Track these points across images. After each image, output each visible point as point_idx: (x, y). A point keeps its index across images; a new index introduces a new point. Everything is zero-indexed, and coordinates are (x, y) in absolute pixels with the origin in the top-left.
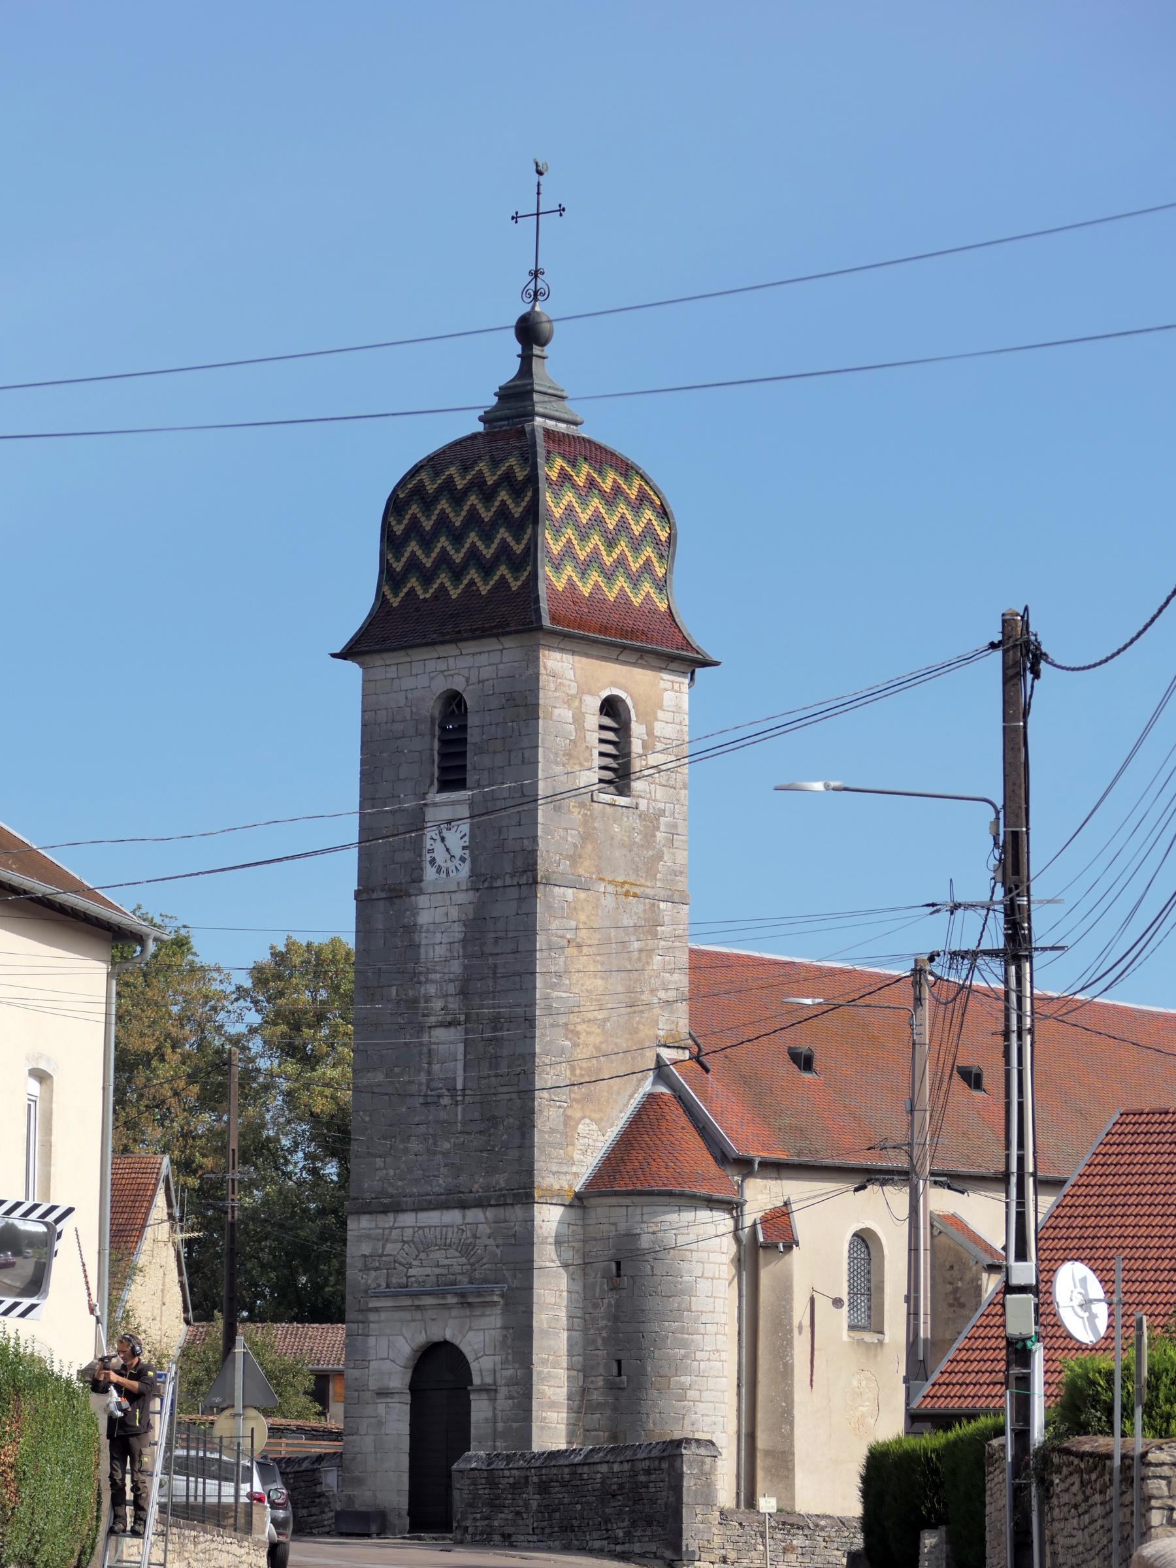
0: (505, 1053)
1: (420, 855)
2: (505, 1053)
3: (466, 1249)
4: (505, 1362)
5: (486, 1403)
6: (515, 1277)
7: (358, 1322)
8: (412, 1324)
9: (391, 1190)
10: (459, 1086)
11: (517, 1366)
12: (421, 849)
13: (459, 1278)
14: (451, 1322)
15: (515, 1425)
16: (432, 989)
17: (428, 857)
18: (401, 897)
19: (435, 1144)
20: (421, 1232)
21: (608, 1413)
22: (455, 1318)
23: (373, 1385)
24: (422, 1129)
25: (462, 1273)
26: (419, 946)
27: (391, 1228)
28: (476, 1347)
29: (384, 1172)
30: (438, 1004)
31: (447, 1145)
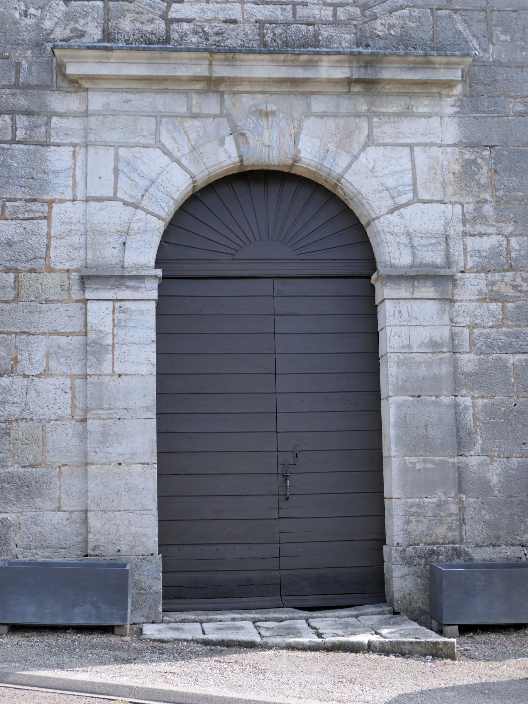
5: (432, 307)
6: (489, 36)
7: (12, 113)
8: (189, 123)
11: (510, 228)
13: (325, 32)
14: (309, 124)
15: (512, 359)
22: (323, 115)
23: (65, 256)
25: (336, 23)
28: (390, 182)
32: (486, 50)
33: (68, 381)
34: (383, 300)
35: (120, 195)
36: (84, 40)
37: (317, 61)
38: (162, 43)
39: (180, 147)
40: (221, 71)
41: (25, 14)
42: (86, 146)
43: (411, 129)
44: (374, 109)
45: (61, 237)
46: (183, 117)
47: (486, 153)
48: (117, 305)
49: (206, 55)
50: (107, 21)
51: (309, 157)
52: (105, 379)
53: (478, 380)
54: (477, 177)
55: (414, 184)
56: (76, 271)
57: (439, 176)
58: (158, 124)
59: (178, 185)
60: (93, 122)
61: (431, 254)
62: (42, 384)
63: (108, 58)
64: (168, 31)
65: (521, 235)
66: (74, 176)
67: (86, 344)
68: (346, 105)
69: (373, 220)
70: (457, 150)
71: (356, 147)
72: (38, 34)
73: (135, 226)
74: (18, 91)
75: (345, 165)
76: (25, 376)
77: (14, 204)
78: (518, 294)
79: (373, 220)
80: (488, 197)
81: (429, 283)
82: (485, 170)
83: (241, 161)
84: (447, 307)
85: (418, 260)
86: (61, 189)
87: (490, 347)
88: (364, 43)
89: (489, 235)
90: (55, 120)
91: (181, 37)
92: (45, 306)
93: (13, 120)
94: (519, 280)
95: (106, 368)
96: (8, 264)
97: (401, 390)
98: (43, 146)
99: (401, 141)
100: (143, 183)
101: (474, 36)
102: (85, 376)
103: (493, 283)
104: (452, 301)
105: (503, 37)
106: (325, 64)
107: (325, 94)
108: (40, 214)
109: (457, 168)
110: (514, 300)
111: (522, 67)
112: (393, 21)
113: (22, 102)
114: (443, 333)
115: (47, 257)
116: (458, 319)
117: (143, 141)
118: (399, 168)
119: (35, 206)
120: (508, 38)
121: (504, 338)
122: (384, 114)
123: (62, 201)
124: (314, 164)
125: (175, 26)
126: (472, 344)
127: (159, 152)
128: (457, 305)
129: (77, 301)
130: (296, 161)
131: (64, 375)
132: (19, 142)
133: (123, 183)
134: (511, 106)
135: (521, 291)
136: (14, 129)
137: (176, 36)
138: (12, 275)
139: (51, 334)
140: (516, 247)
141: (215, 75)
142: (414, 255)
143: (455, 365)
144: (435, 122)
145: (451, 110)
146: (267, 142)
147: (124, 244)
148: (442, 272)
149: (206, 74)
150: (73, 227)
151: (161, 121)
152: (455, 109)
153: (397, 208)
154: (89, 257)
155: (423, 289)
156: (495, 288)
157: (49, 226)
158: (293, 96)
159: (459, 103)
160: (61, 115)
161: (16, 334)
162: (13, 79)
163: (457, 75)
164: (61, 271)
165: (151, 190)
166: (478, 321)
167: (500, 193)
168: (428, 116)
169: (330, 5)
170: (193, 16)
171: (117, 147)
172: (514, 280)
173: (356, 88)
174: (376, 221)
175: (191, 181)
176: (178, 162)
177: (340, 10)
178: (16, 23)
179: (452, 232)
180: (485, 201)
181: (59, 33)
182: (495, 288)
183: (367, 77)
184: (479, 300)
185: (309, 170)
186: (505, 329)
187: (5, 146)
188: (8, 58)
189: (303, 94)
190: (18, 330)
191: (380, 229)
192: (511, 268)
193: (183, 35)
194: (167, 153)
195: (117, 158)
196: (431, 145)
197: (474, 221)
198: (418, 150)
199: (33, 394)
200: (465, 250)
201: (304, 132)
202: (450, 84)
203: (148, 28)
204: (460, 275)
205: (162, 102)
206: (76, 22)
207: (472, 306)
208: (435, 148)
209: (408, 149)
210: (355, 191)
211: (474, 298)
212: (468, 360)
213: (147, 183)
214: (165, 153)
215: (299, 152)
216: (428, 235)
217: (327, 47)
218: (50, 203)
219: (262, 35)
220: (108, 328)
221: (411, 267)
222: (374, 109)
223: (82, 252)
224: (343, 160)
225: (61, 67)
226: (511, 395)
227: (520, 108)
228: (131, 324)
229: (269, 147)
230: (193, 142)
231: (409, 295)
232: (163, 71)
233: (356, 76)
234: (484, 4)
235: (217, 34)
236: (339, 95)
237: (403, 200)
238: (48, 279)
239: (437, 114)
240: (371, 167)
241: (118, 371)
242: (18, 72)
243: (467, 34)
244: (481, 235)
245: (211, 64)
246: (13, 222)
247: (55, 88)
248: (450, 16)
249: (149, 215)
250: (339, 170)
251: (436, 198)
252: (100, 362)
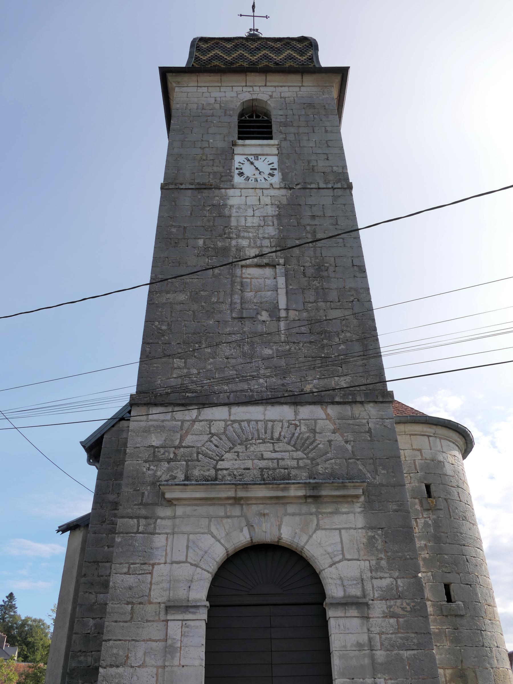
0: (334, 286)
1: (230, 170)
2: (334, 286)
3: (301, 444)
4: (376, 569)
5: (356, 622)
6: (376, 472)
7: (138, 517)
8: (225, 521)
9: (192, 387)
10: (282, 304)
11: (396, 574)
13: (293, 472)
14: (286, 519)
16: (245, 243)
17: (237, 172)
18: (210, 189)
19: (252, 348)
20: (236, 425)
21: (447, 645)
22: (293, 515)
23: (158, 595)
25: (298, 467)
26: (230, 216)
27: (194, 421)
28: (330, 550)
29: (185, 371)
31: (268, 352)
32: (375, 478)
33: (155, 670)
34: (329, 618)
35: (189, 560)
36: (176, 480)
37: (288, 487)
38: (214, 481)
39: (220, 533)
40: (241, 494)
41: (149, 469)
42: (173, 534)
43: (339, 520)
44: (319, 510)
45: (157, 584)
46: (222, 517)
47: (380, 532)
48: (184, 623)
49: (234, 486)
50: (187, 471)
51: (286, 537)
52: (175, 669)
54: (376, 545)
55: (343, 550)
56: (164, 603)
57: (355, 546)
58: (210, 521)
59: (219, 554)
60: (177, 521)
61: (354, 589)
62: (141, 672)
63: (186, 489)
64: (216, 475)
65: (403, 578)
66: (166, 550)
67: (166, 647)
68: (305, 509)
69: (322, 571)
70: (364, 531)
71: (311, 531)
72: (154, 479)
73: (196, 577)
74: (141, 507)
75: (305, 541)
76: (132, 667)
77: (134, 566)
78: (405, 613)
79: (322, 571)
80: (382, 556)
81: (354, 607)
82: (380, 541)
83: (252, 540)
84: (365, 622)
85: (347, 594)
86: (159, 557)
87: (392, 646)
88: (313, 477)
89: (385, 578)
90: (159, 521)
91: (223, 477)
92: (146, 624)
93: (138, 521)
94: (405, 604)
95: (176, 662)
96: (128, 600)
97: (342, 675)
98: (152, 534)
99: (334, 527)
100: (201, 553)
101: (368, 471)
102: (164, 667)
103: (390, 607)
104: (368, 618)
105: (383, 472)
106: (292, 489)
107: (294, 503)
108: (148, 571)
109: (365, 540)
110: (403, 616)
111: (394, 486)
112: (327, 465)
113: (143, 512)
114: (364, 638)
115: (149, 595)
116: (373, 629)
117: (202, 531)
118: (334, 542)
119: (145, 567)
120: (385, 472)
121: (400, 641)
122: (324, 513)
123: (159, 564)
124: (289, 541)
125: (220, 472)
126: (382, 645)
127: (209, 536)
128: (371, 620)
129: (163, 621)
130: (280, 539)
131: (153, 666)
132: (140, 533)
133: (191, 554)
134: (390, 506)
135: (406, 611)
136: (139, 526)
137: (220, 477)
138: (130, 606)
139: (148, 641)
140: (401, 585)
141: (238, 496)
142: (345, 591)
143: (372, 658)
144: (351, 516)
145: (359, 510)
146: (264, 530)
147: (190, 587)
148: (361, 601)
149: (233, 495)
150: (164, 578)
151: (211, 520)
152: (361, 509)
153: (334, 564)
154: (171, 595)
155: (351, 611)
156: (392, 610)
157: (152, 578)
158: (277, 505)
159: (363, 506)
160: (162, 518)
161: (129, 641)
162: (140, 501)
163: (360, 492)
164: (156, 603)
165: (205, 557)
166: (384, 630)
167: (389, 554)
168: (347, 513)
169: (295, 459)
170: (229, 467)
171: (189, 534)
172: (402, 605)
173: (309, 500)
174: (323, 572)
175: (225, 552)
176: (219, 541)
177: (300, 461)
178: (144, 473)
179: (365, 577)
180: (382, 559)
181: (164, 478)
182: (392, 610)
183: (314, 494)
184: (383, 617)
185: (287, 544)
186: (400, 635)
187: (133, 535)
188: (138, 490)
189: (283, 504)
190: (131, 639)
191: (325, 576)
192: (399, 597)
193: (224, 476)
194: (214, 537)
195: (188, 540)
196: (350, 528)
197: (376, 570)
198: (343, 531)
199: (135, 678)
200: (373, 587)
201: (284, 523)
202: (357, 497)
203: (207, 473)
204: (371, 602)
205: (212, 510)
206: (173, 472)
207: (380, 621)
208: (352, 530)
209: (338, 531)
210: (311, 555)
211: (380, 616)
212: (380, 655)
213: (203, 553)
214: (212, 537)
215: (281, 534)
216: (352, 579)
217: (294, 480)
218: (153, 565)
219: (262, 475)
220: (178, 637)
221: (344, 597)
222: (319, 510)
223: (168, 592)
224: (304, 538)
225: (163, 494)
226: (408, 677)
227: (395, 507)
228: (191, 635)
229: (265, 532)
230: (227, 531)
231: (343, 615)
232: (213, 495)
233: (308, 494)
234: (372, 456)
235: (240, 475)
236: (301, 504)
237: (337, 559)
238: (150, 608)
239: (352, 512)
240: (319, 541)
241: (182, 664)
242: (143, 497)
243: (364, 470)
244: (381, 578)
245: (236, 491)
246: (134, 576)
247: (160, 504)
248: (355, 462)
249: (203, 571)
250: (302, 544)
251: (354, 558)
252: (173, 658)
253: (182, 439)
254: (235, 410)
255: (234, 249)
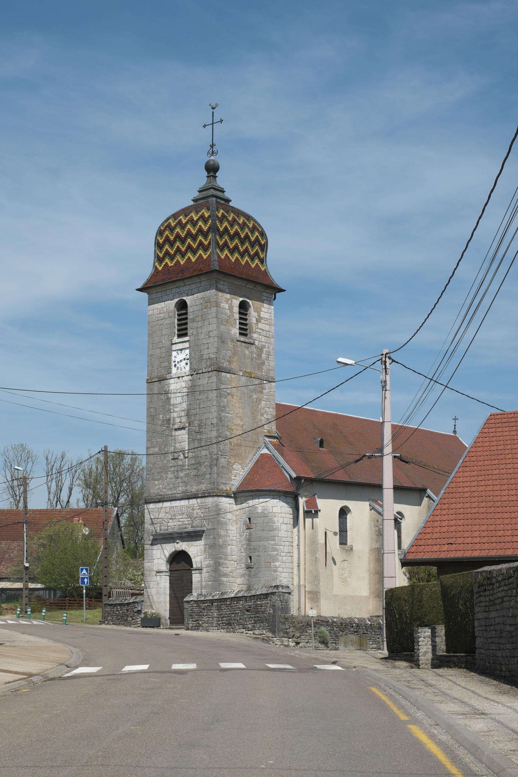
1: (171, 363)
3: (190, 516)
4: (205, 558)
11: (210, 559)
12: (171, 361)
15: (210, 583)
16: (175, 415)
19: (178, 474)
21: (247, 577)
23: (156, 569)
24: (173, 469)
25: (189, 524)
30: (178, 420)
53: (205, 587)
62: (153, 590)
253: (159, 515)
254: (172, 502)
255: (172, 419)
